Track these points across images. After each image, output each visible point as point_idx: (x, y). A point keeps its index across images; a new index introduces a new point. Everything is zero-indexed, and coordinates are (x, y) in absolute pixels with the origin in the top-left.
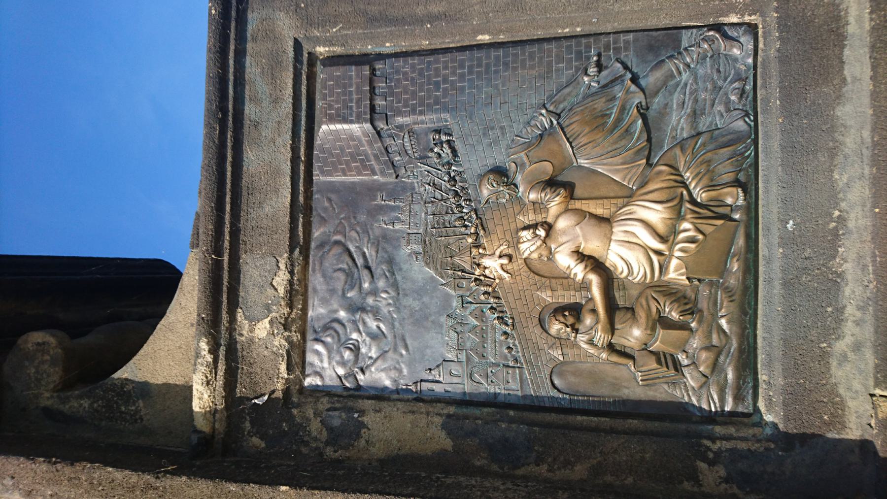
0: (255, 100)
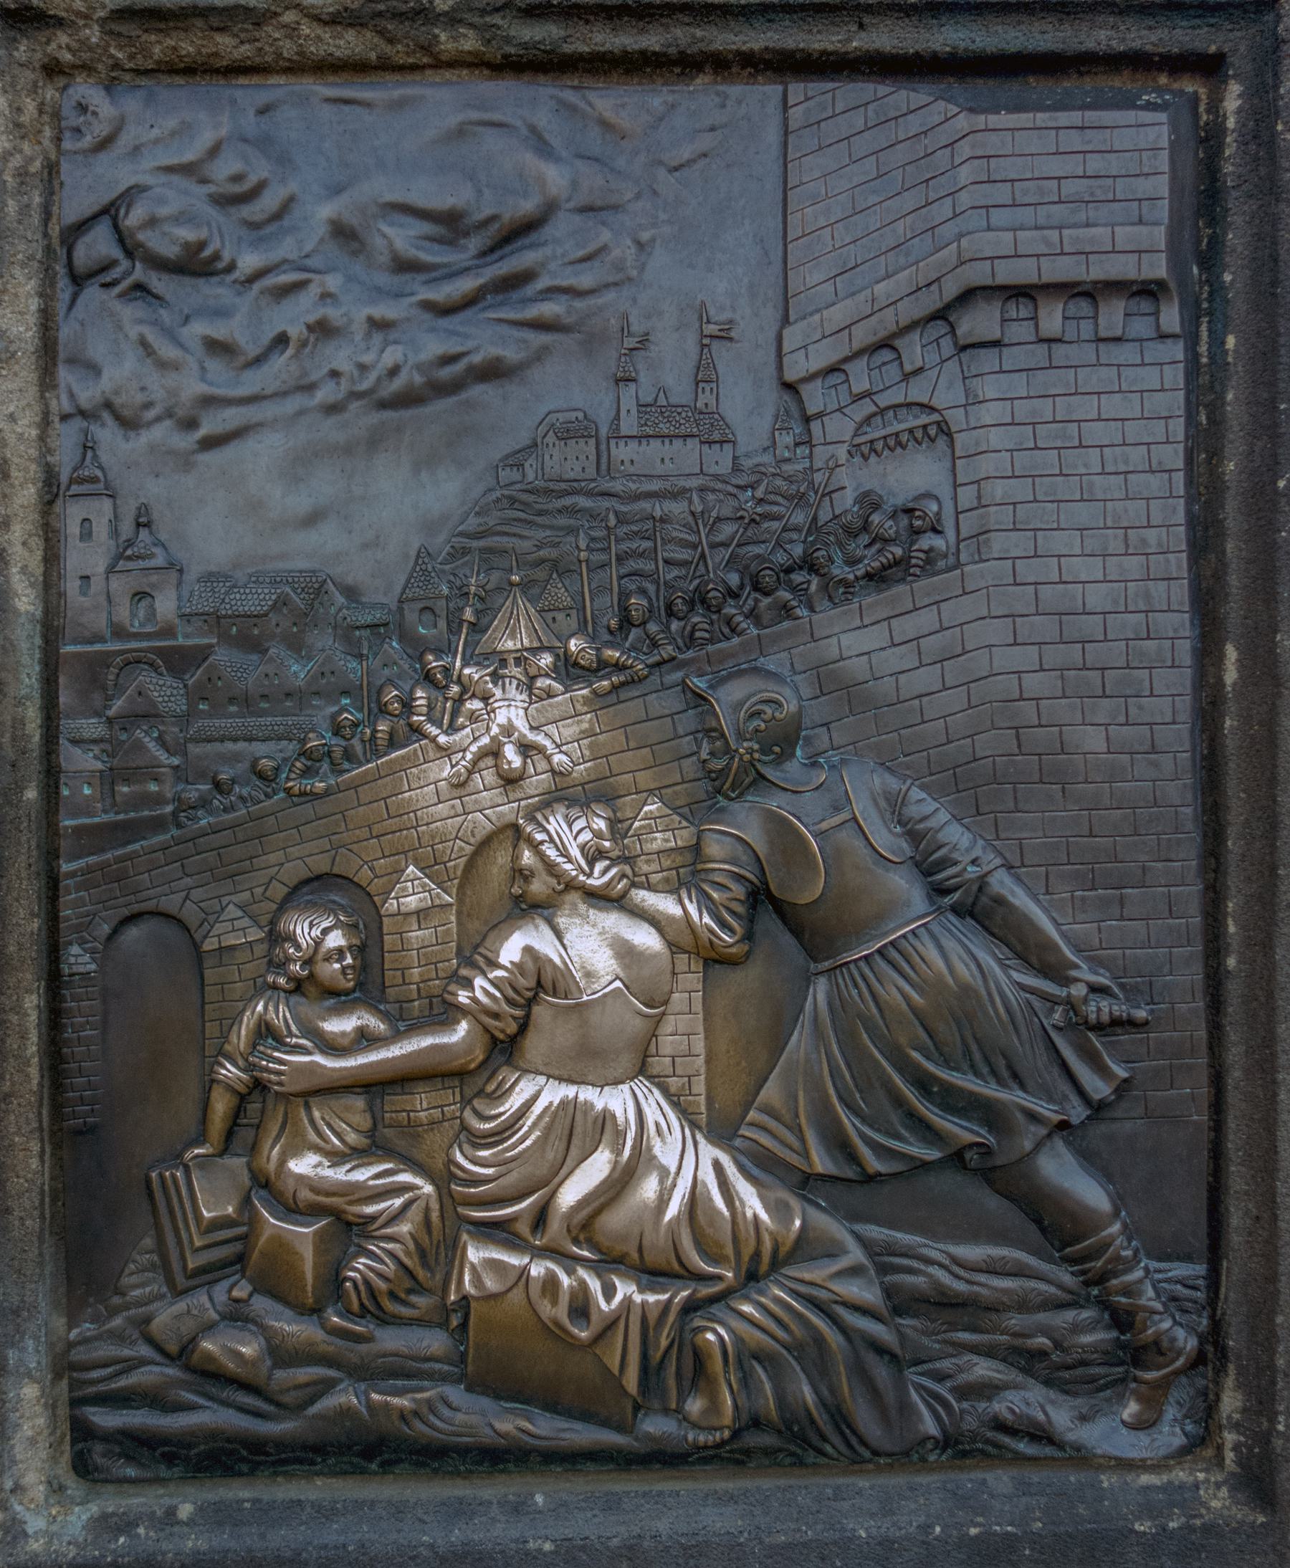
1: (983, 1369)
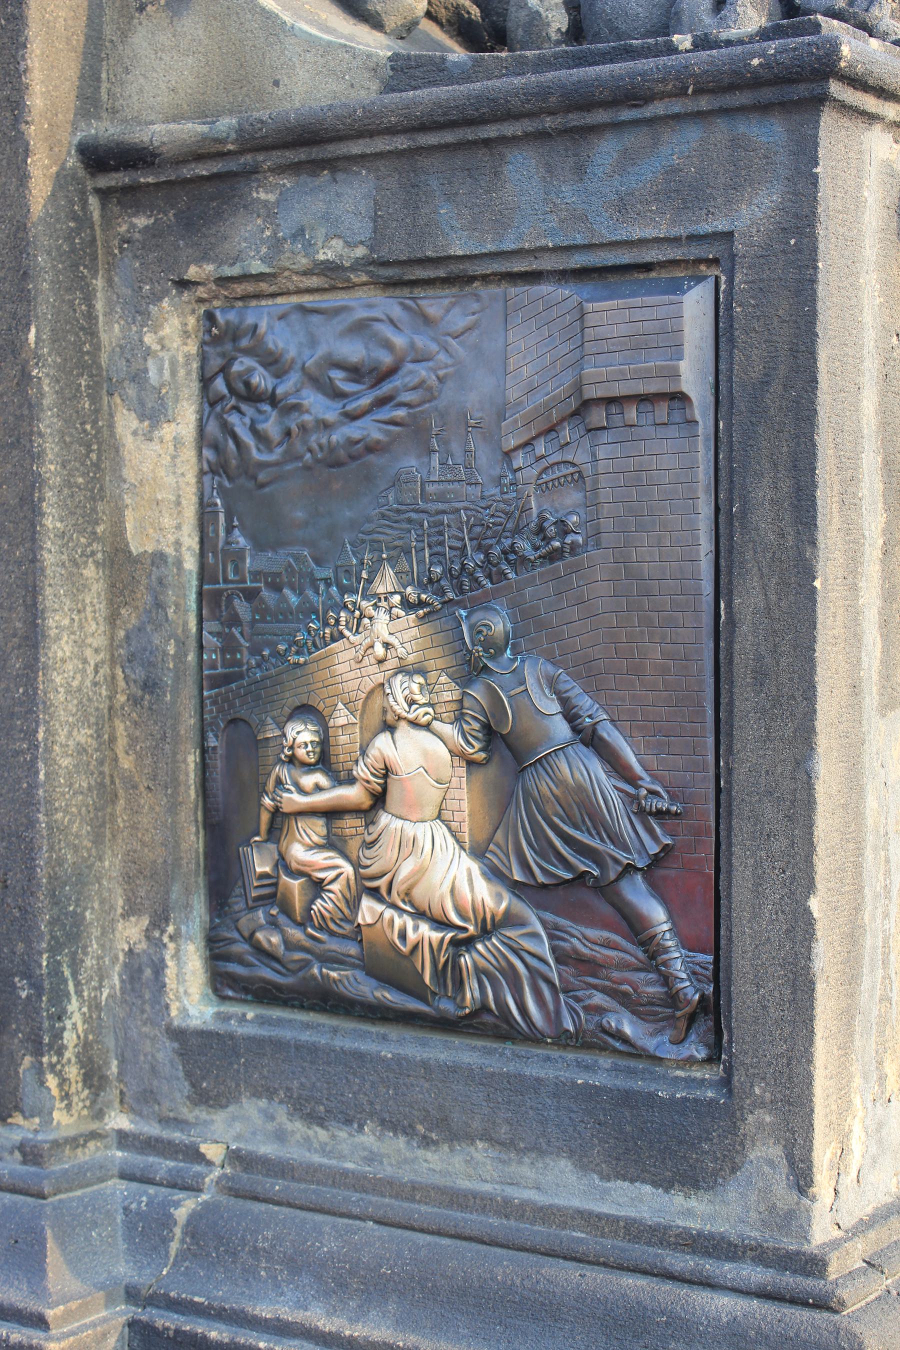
0: (627, 158)
1: (598, 999)
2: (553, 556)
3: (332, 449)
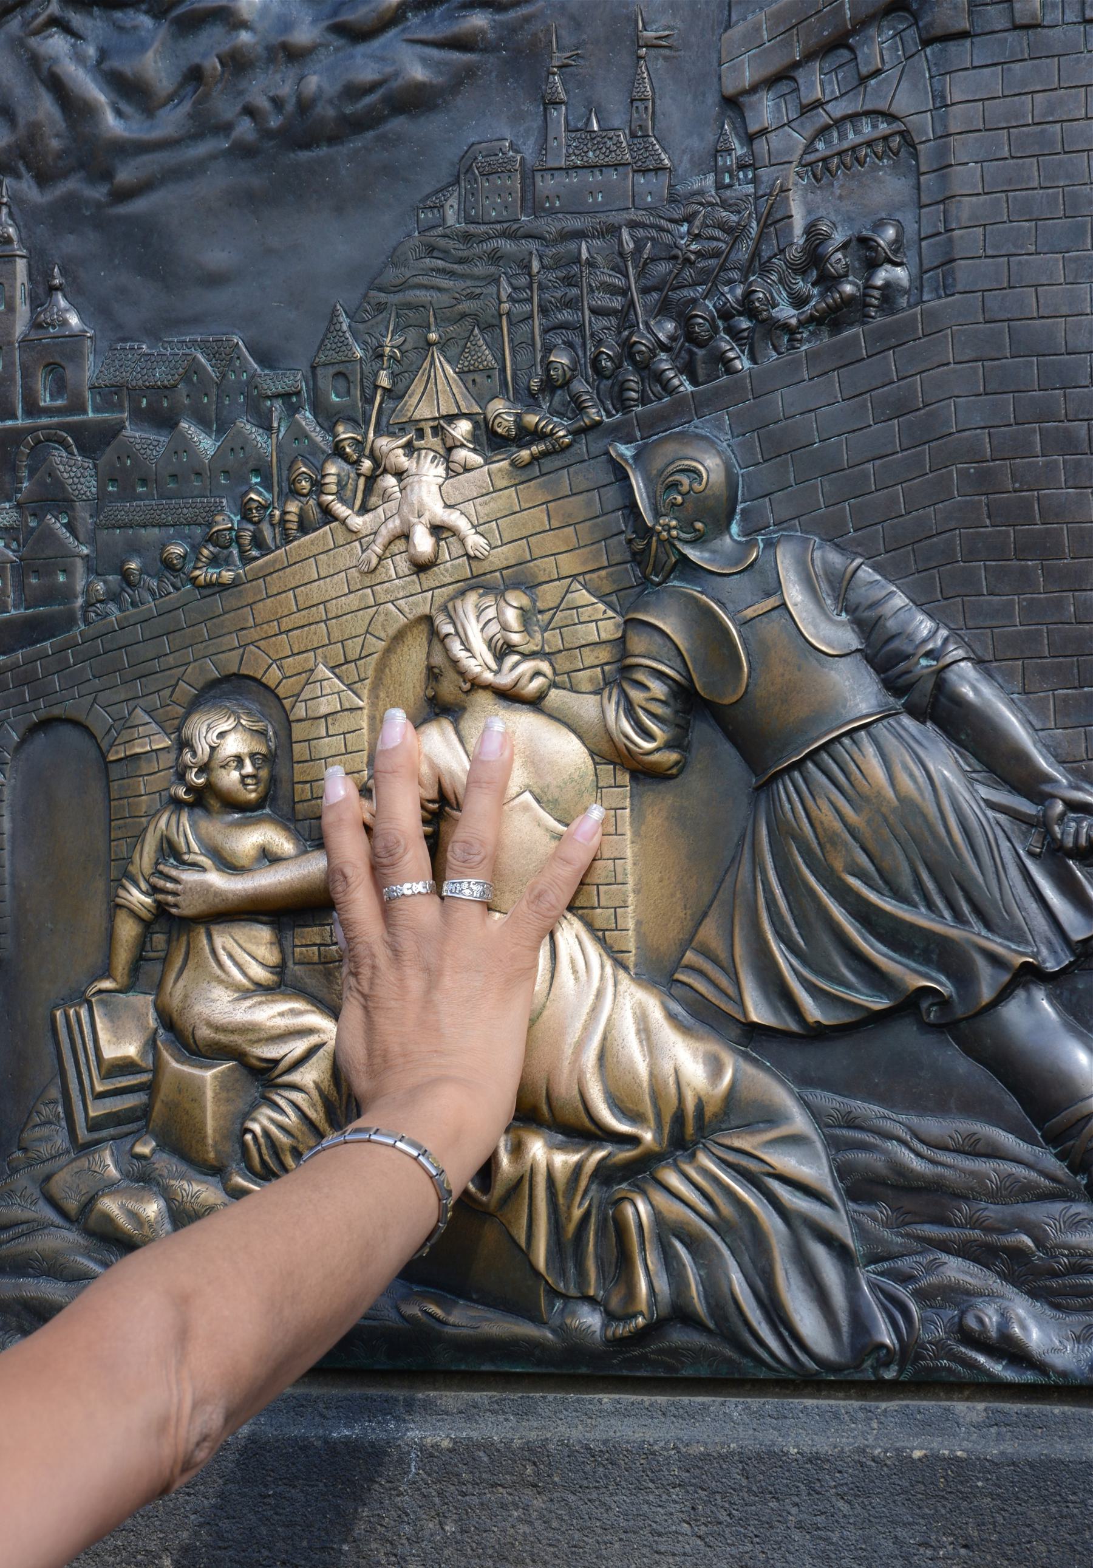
2: (833, 318)
3: (304, 106)
